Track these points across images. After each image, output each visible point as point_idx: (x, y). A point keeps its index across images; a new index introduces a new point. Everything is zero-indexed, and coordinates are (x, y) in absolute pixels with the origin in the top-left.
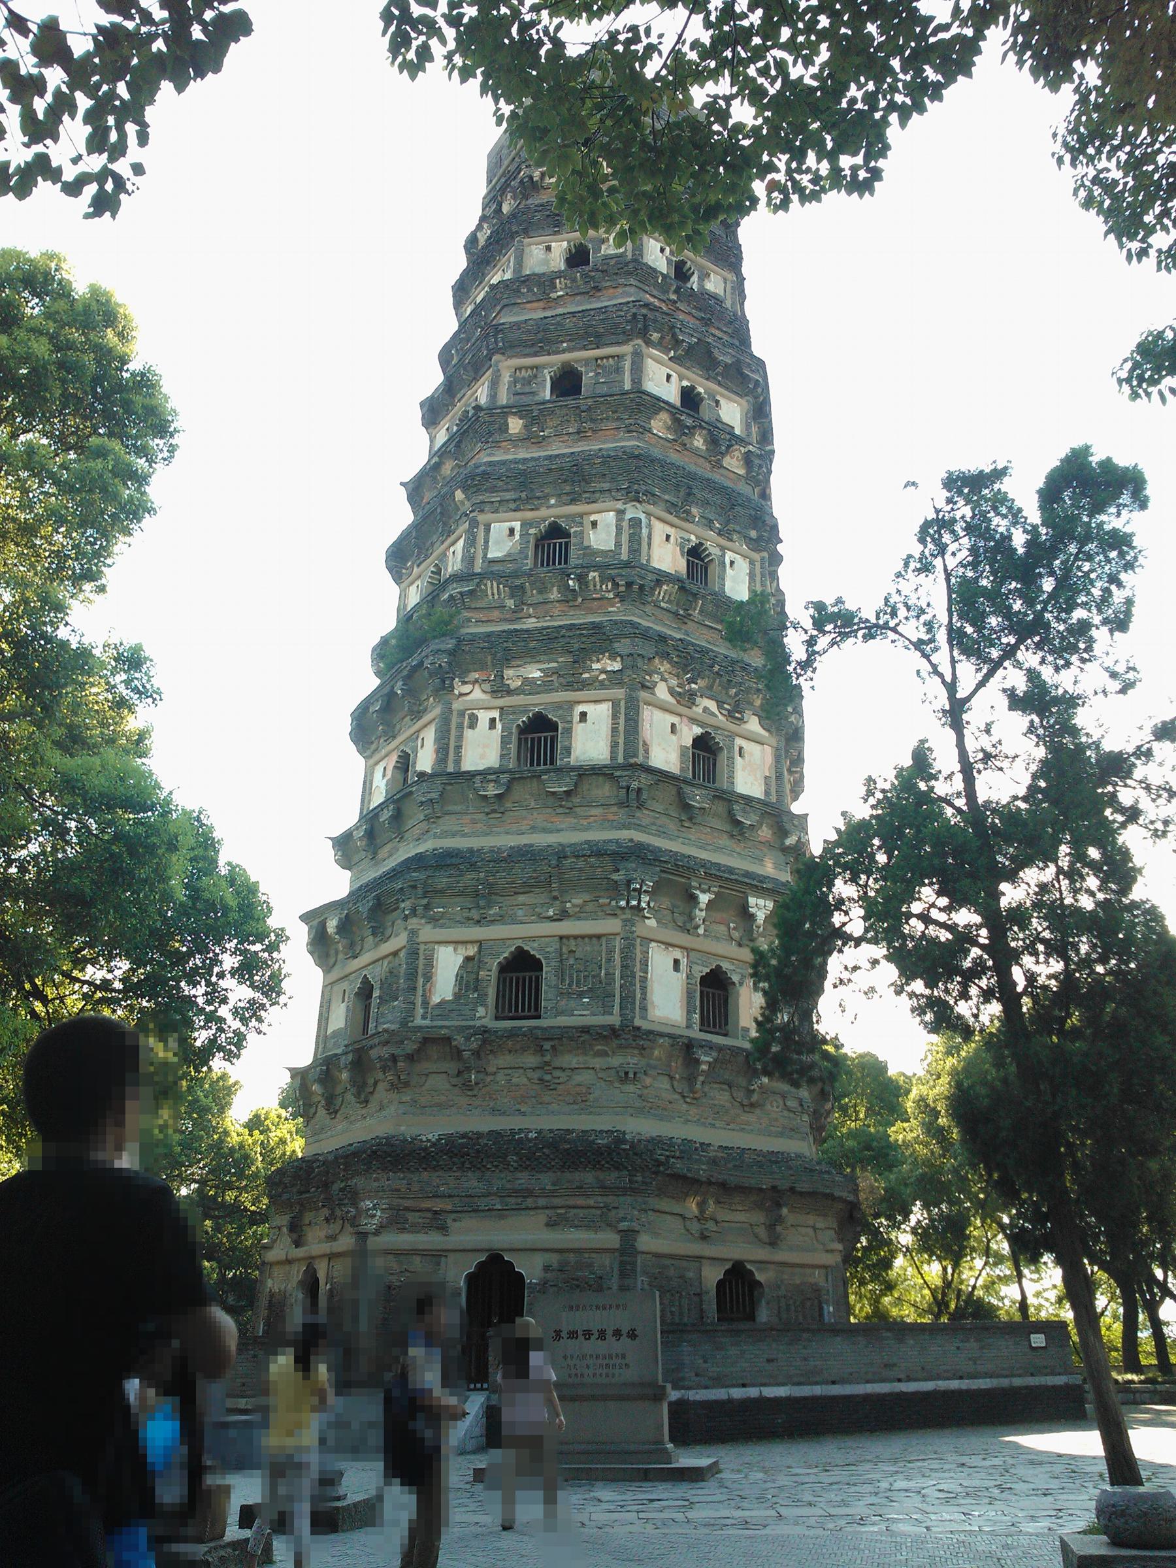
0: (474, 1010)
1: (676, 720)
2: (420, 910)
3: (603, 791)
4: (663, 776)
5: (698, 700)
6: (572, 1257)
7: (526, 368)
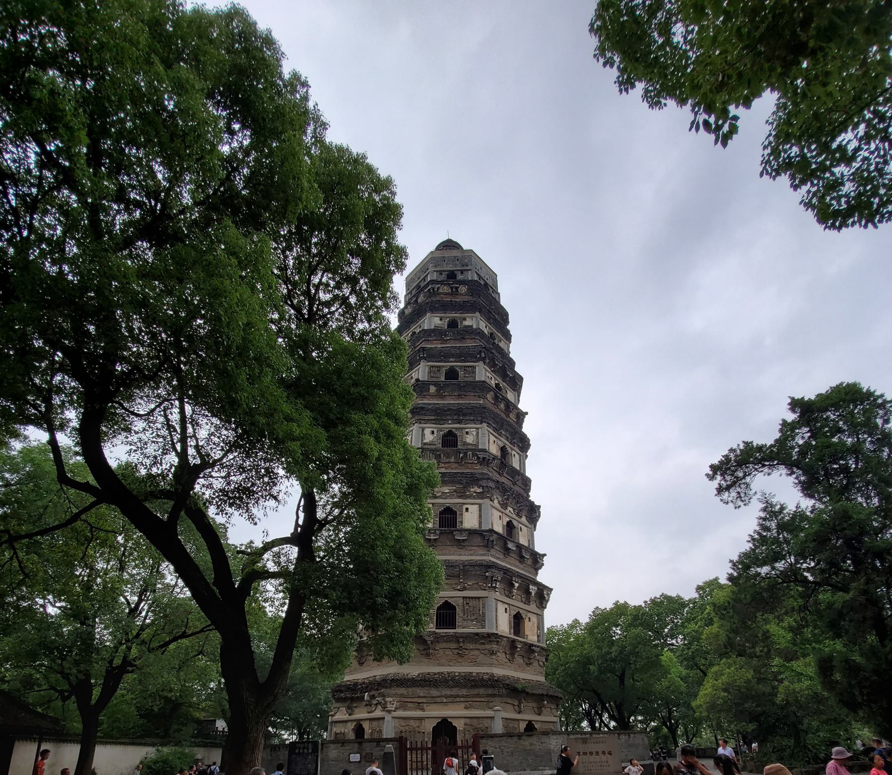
3: (478, 540)
6: (475, 720)
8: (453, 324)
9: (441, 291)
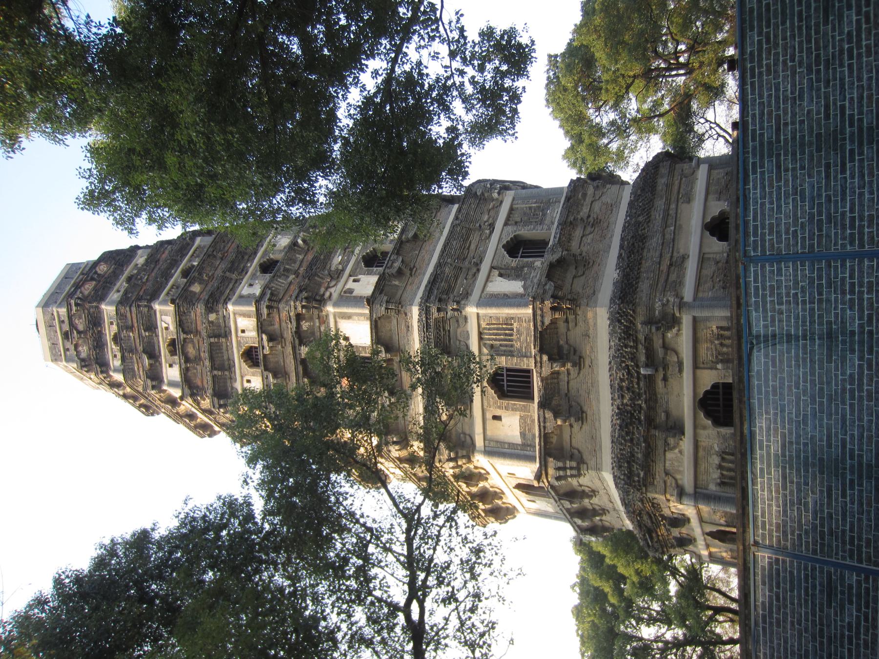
7: (170, 290)
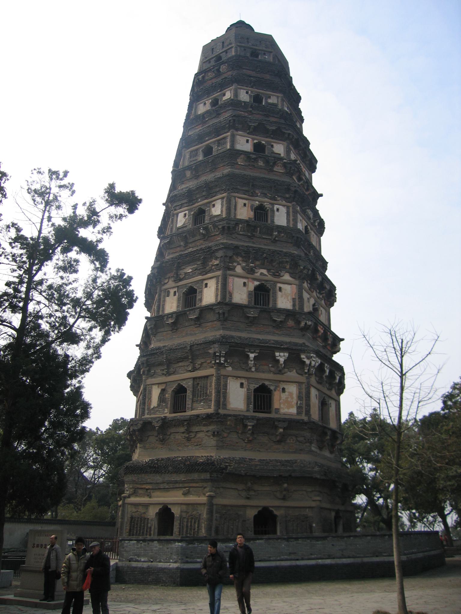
0: (164, 410)
1: (245, 280)
2: (146, 372)
4: (239, 307)
5: (256, 271)
8: (215, 103)
9: (207, 78)
